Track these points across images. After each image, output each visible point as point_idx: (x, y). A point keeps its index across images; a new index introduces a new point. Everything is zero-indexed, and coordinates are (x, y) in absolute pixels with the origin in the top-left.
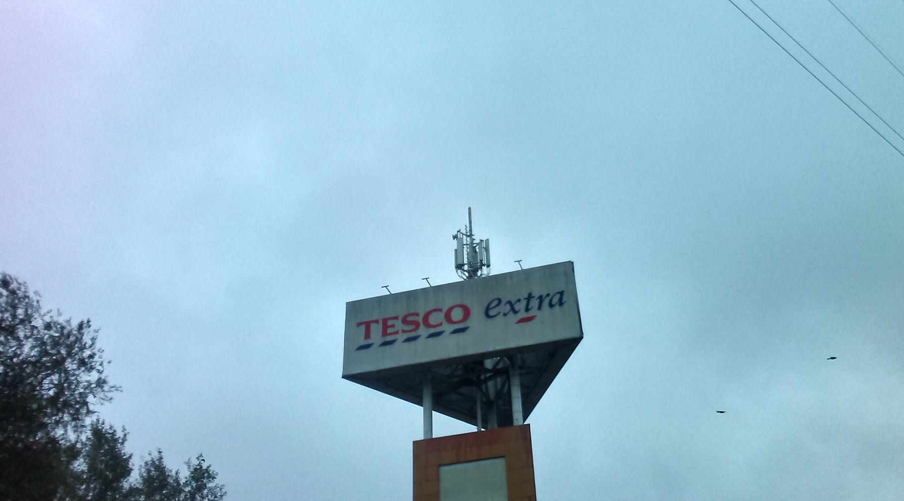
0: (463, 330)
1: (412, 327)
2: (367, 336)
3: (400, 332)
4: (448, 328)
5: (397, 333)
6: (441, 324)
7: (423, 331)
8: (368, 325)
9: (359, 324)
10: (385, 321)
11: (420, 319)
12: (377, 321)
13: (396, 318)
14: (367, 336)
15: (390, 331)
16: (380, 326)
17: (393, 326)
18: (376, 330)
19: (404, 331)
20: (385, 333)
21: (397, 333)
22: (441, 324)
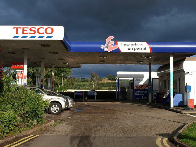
0: (51, 37)
1: (33, 32)
2: (17, 33)
3: (29, 33)
4: (46, 35)
5: (28, 33)
6: (43, 33)
7: (37, 35)
9: (14, 28)
10: (24, 28)
11: (36, 30)
12: (21, 28)
13: (28, 28)
14: (17, 33)
15: (25, 32)
16: (22, 30)
17: (26, 31)
18: (20, 31)
19: (30, 33)
20: (23, 33)
21: (28, 33)
22: (43, 33)
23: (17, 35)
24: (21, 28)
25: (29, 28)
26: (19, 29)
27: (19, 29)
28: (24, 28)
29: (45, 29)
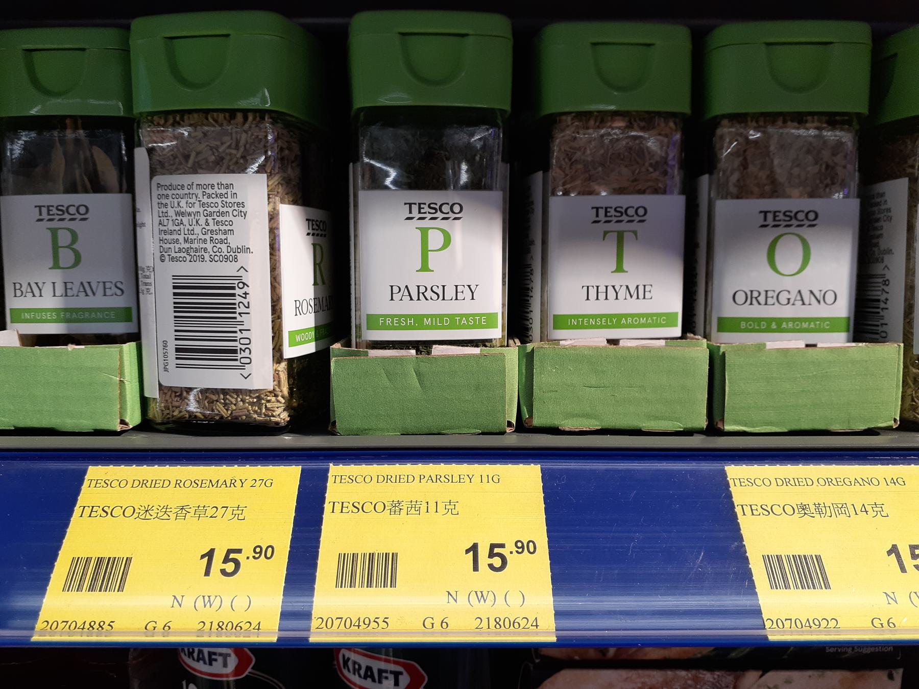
5: (425, 213)
6: (448, 213)
8: (410, 204)
9: (405, 204)
10: (420, 204)
11: (437, 207)
12: (415, 204)
13: (425, 204)
15: (422, 211)
17: (423, 208)
19: (429, 213)
21: (425, 213)
22: (448, 213)
23: (411, 216)
24: (415, 204)
25: (427, 204)
26: (413, 205)
27: (413, 205)
28: (420, 204)
29: (450, 204)
